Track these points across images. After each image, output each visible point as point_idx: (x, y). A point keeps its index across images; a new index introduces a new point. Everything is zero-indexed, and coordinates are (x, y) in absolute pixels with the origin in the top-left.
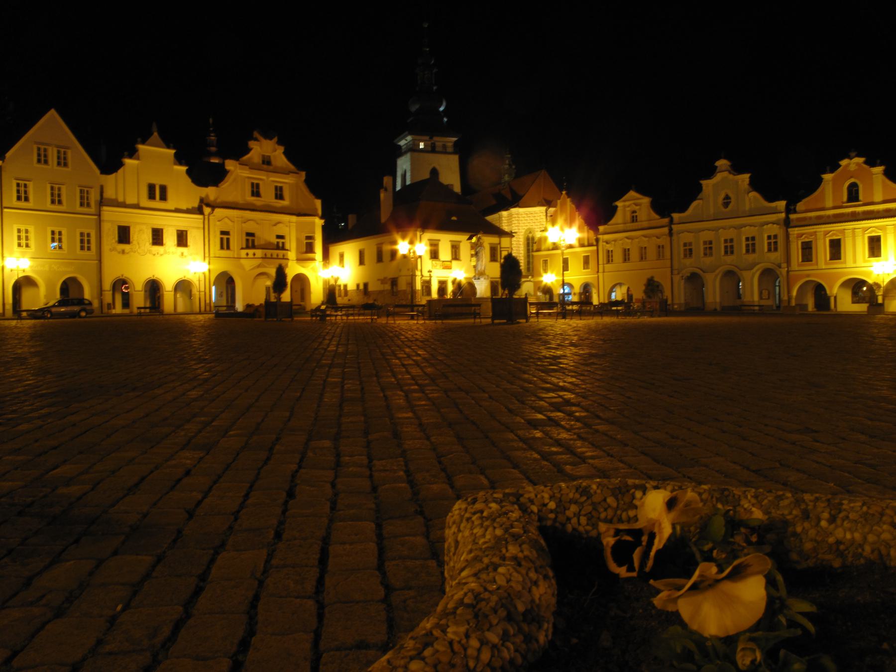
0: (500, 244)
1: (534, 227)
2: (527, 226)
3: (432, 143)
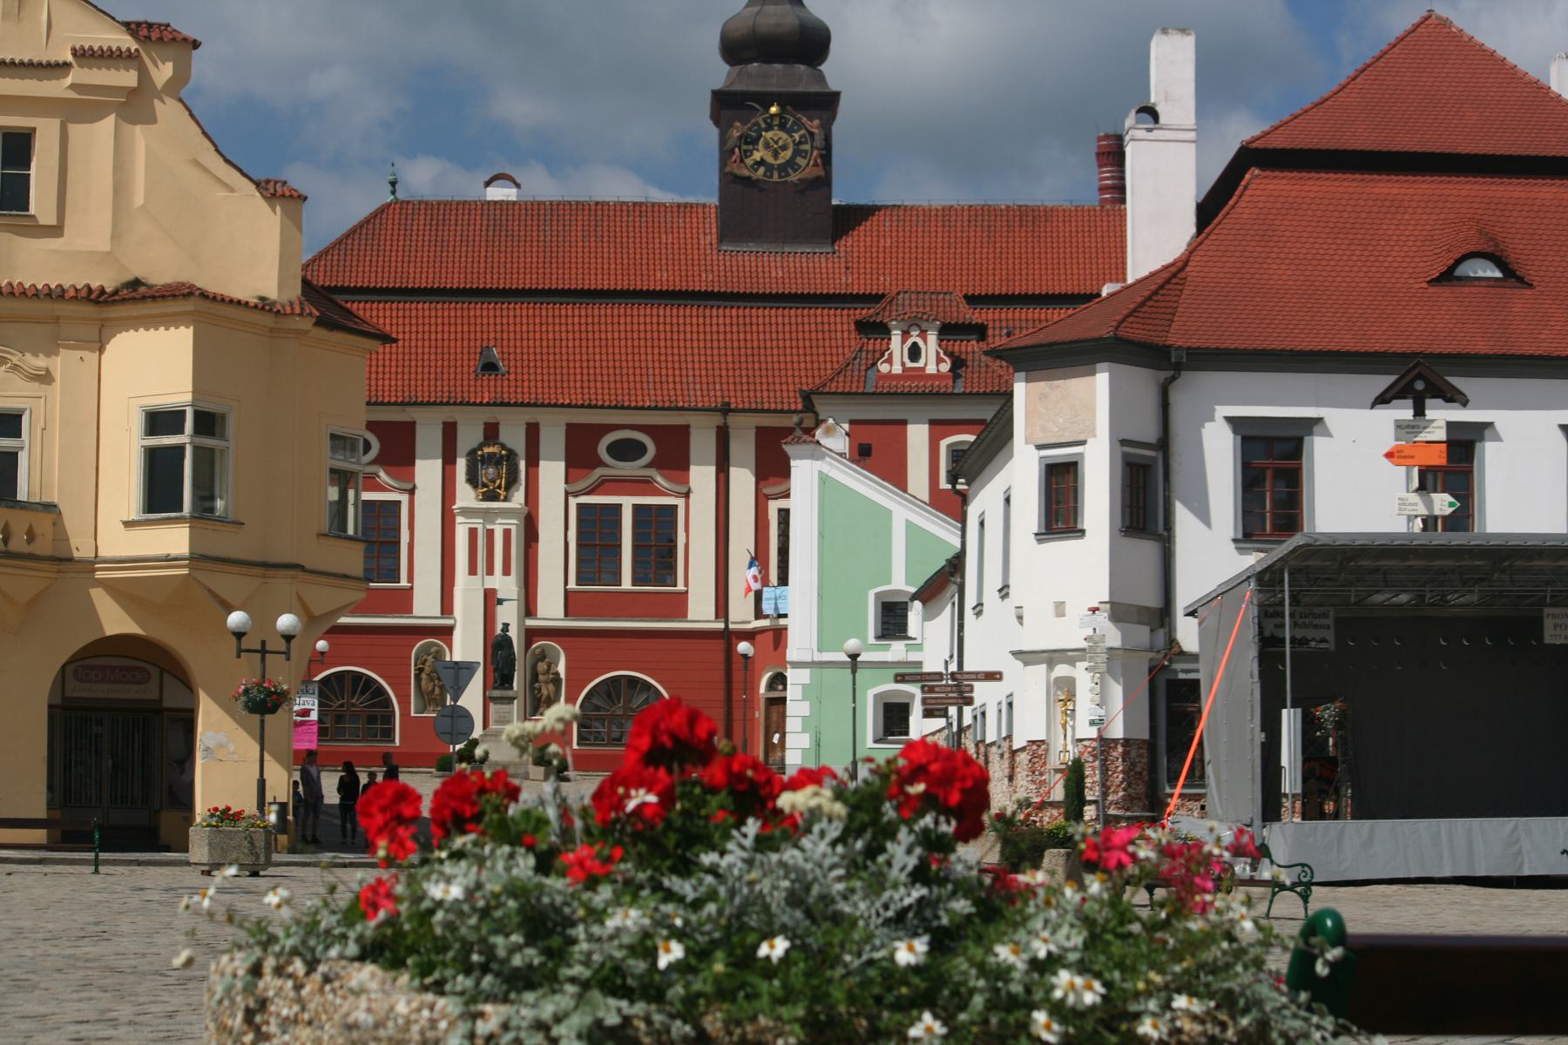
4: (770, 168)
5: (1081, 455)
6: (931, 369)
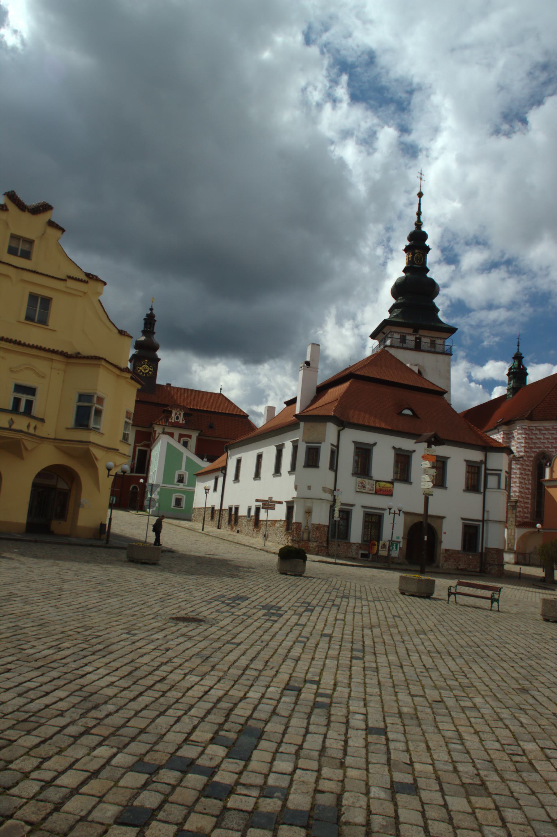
0: (485, 463)
1: (550, 450)
2: (540, 447)
3: (416, 338)
4: (143, 373)
5: (320, 447)
6: (181, 422)
